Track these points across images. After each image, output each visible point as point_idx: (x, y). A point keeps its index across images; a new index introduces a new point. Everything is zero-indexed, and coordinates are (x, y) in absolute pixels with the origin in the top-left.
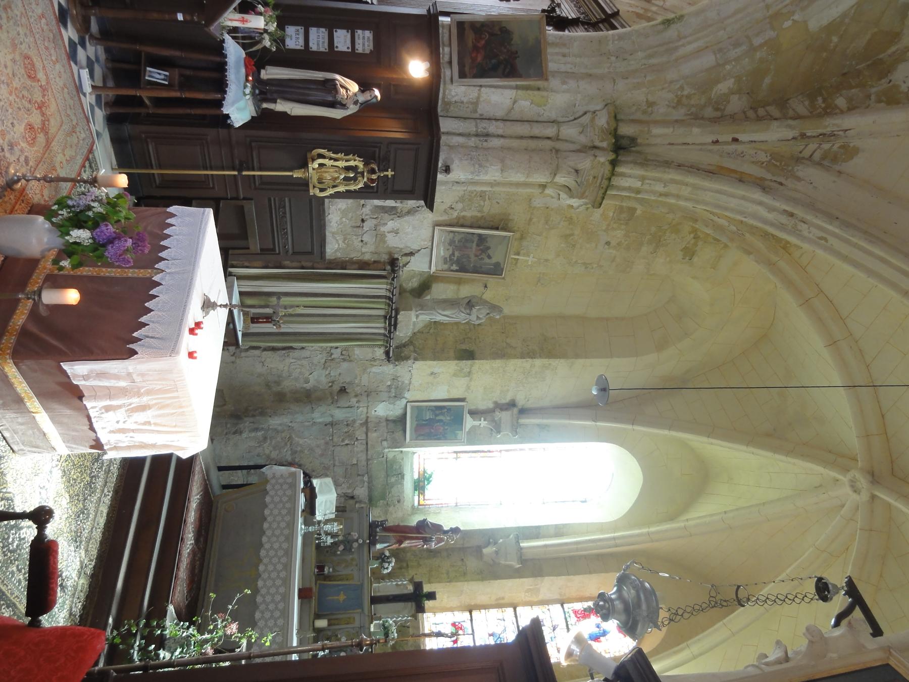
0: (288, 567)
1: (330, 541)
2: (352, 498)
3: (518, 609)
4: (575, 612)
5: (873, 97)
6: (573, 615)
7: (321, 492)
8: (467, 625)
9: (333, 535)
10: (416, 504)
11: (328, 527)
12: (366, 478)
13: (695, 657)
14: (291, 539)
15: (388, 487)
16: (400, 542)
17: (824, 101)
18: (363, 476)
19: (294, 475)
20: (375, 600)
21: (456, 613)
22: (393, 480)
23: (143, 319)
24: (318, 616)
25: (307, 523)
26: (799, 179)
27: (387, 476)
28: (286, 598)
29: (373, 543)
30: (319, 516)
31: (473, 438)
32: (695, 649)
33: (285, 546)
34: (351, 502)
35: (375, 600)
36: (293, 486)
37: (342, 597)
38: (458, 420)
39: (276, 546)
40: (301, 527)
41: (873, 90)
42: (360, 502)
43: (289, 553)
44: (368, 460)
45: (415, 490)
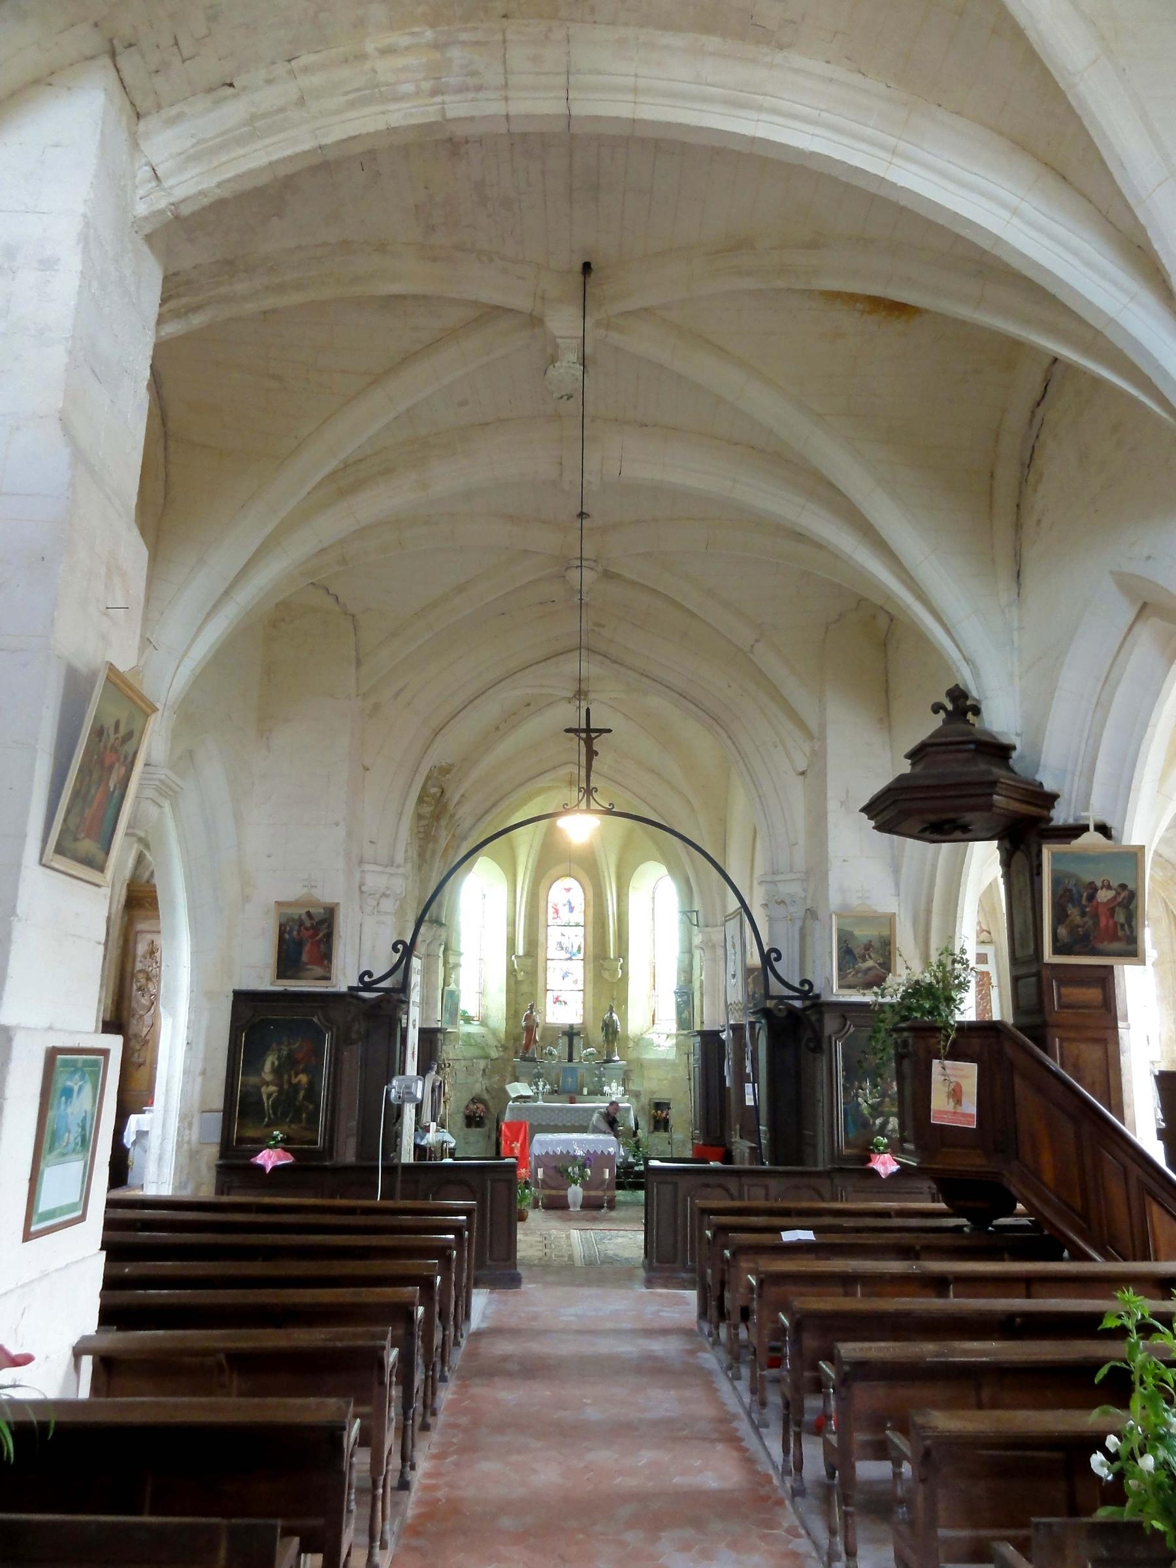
0: (560, 1109)
1: (548, 1087)
2: (484, 1070)
3: (548, 957)
4: (554, 918)
5: (439, 777)
6: (555, 921)
7: (519, 1092)
8: (556, 994)
9: (544, 1086)
10: (478, 1023)
11: (541, 1088)
12: (475, 1061)
13: (608, 869)
14: (544, 1109)
15: (477, 1045)
16: (536, 1042)
17: (428, 797)
18: (473, 1063)
19: (512, 1109)
20: (570, 1060)
21: (547, 1000)
22: (472, 1041)
23: (599, 1153)
24: (581, 1093)
25: (535, 1100)
26: (460, 818)
27: (471, 1045)
28: (578, 1109)
29: (533, 1060)
30: (531, 1094)
31: (457, 983)
32: (605, 867)
33: (557, 1112)
34: (487, 1071)
35: (570, 1060)
36: (519, 1109)
37: (570, 1080)
38: (452, 993)
39: (548, 1117)
40: (540, 1103)
41: (435, 775)
42: (487, 1065)
43: (552, 1109)
44: (465, 1060)
45: (470, 1023)
